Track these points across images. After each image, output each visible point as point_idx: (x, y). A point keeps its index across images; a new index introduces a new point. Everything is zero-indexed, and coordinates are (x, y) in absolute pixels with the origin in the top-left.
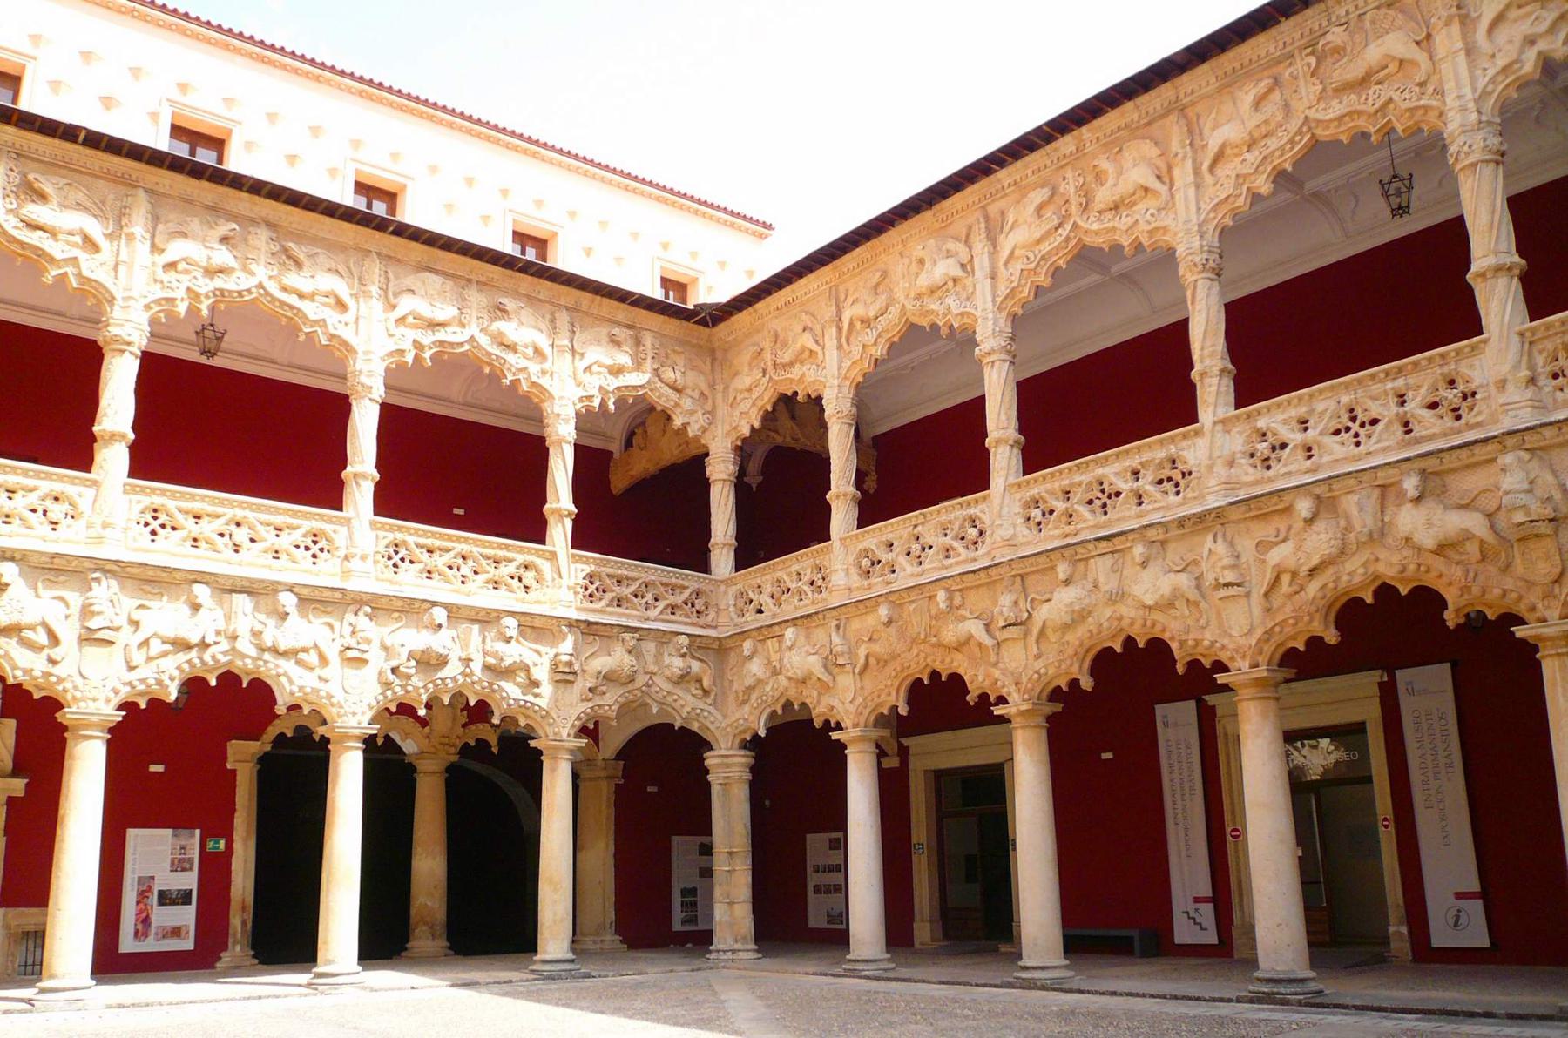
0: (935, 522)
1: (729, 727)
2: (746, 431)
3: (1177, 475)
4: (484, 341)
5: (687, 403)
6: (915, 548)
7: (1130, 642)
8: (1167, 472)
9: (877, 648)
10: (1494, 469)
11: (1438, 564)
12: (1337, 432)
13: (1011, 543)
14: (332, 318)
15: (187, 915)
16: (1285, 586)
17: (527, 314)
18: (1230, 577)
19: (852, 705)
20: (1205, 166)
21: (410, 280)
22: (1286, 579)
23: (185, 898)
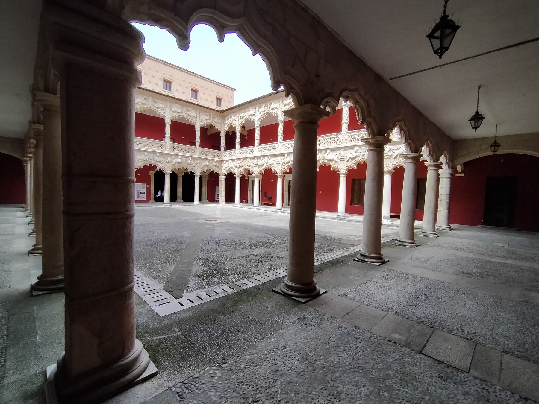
0: (248, 149)
1: (223, 172)
4: (186, 115)
5: (218, 125)
9: (240, 165)
13: (256, 153)
14: (162, 111)
15: (145, 195)
17: (193, 111)
19: (237, 172)
21: (174, 105)
23: (144, 193)
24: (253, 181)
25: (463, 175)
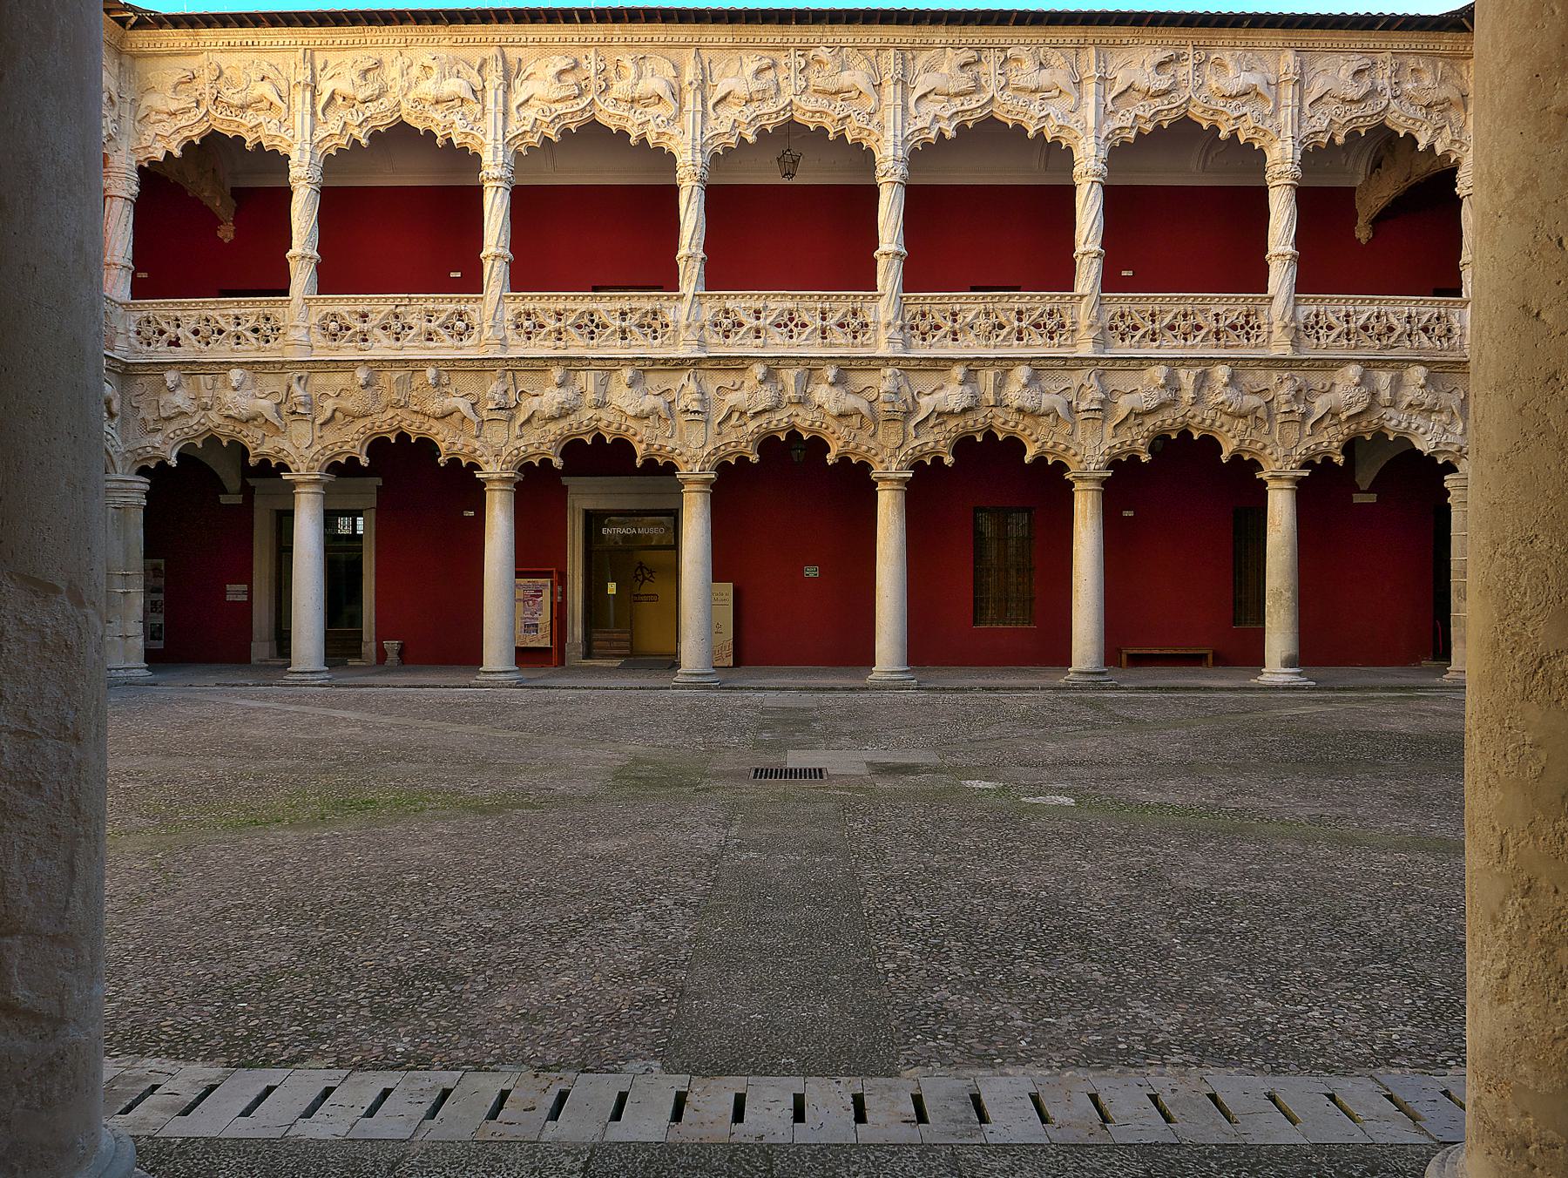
2: (160, 155)
3: (657, 325)
6: (396, 326)
7: (599, 438)
8: (649, 319)
9: (348, 404)
10: (876, 374)
11: (834, 424)
12: (779, 326)
16: (733, 421)
18: (695, 406)
20: (710, 104)
22: (736, 415)
24: (285, 519)
25: (1372, 498)
